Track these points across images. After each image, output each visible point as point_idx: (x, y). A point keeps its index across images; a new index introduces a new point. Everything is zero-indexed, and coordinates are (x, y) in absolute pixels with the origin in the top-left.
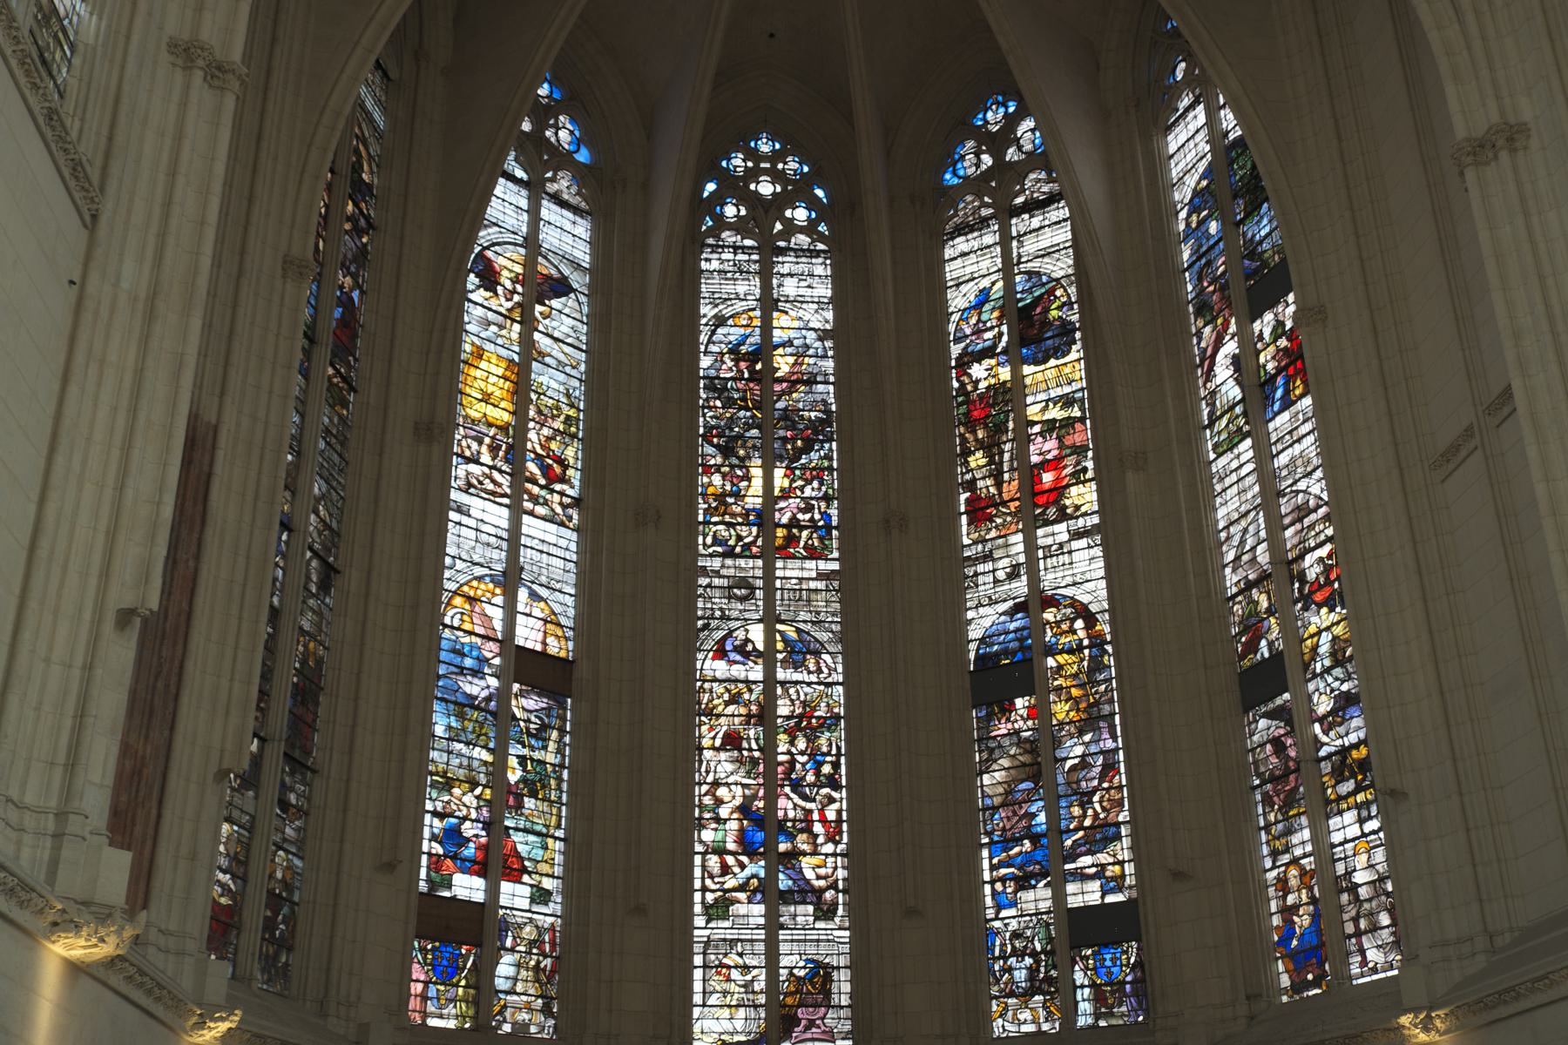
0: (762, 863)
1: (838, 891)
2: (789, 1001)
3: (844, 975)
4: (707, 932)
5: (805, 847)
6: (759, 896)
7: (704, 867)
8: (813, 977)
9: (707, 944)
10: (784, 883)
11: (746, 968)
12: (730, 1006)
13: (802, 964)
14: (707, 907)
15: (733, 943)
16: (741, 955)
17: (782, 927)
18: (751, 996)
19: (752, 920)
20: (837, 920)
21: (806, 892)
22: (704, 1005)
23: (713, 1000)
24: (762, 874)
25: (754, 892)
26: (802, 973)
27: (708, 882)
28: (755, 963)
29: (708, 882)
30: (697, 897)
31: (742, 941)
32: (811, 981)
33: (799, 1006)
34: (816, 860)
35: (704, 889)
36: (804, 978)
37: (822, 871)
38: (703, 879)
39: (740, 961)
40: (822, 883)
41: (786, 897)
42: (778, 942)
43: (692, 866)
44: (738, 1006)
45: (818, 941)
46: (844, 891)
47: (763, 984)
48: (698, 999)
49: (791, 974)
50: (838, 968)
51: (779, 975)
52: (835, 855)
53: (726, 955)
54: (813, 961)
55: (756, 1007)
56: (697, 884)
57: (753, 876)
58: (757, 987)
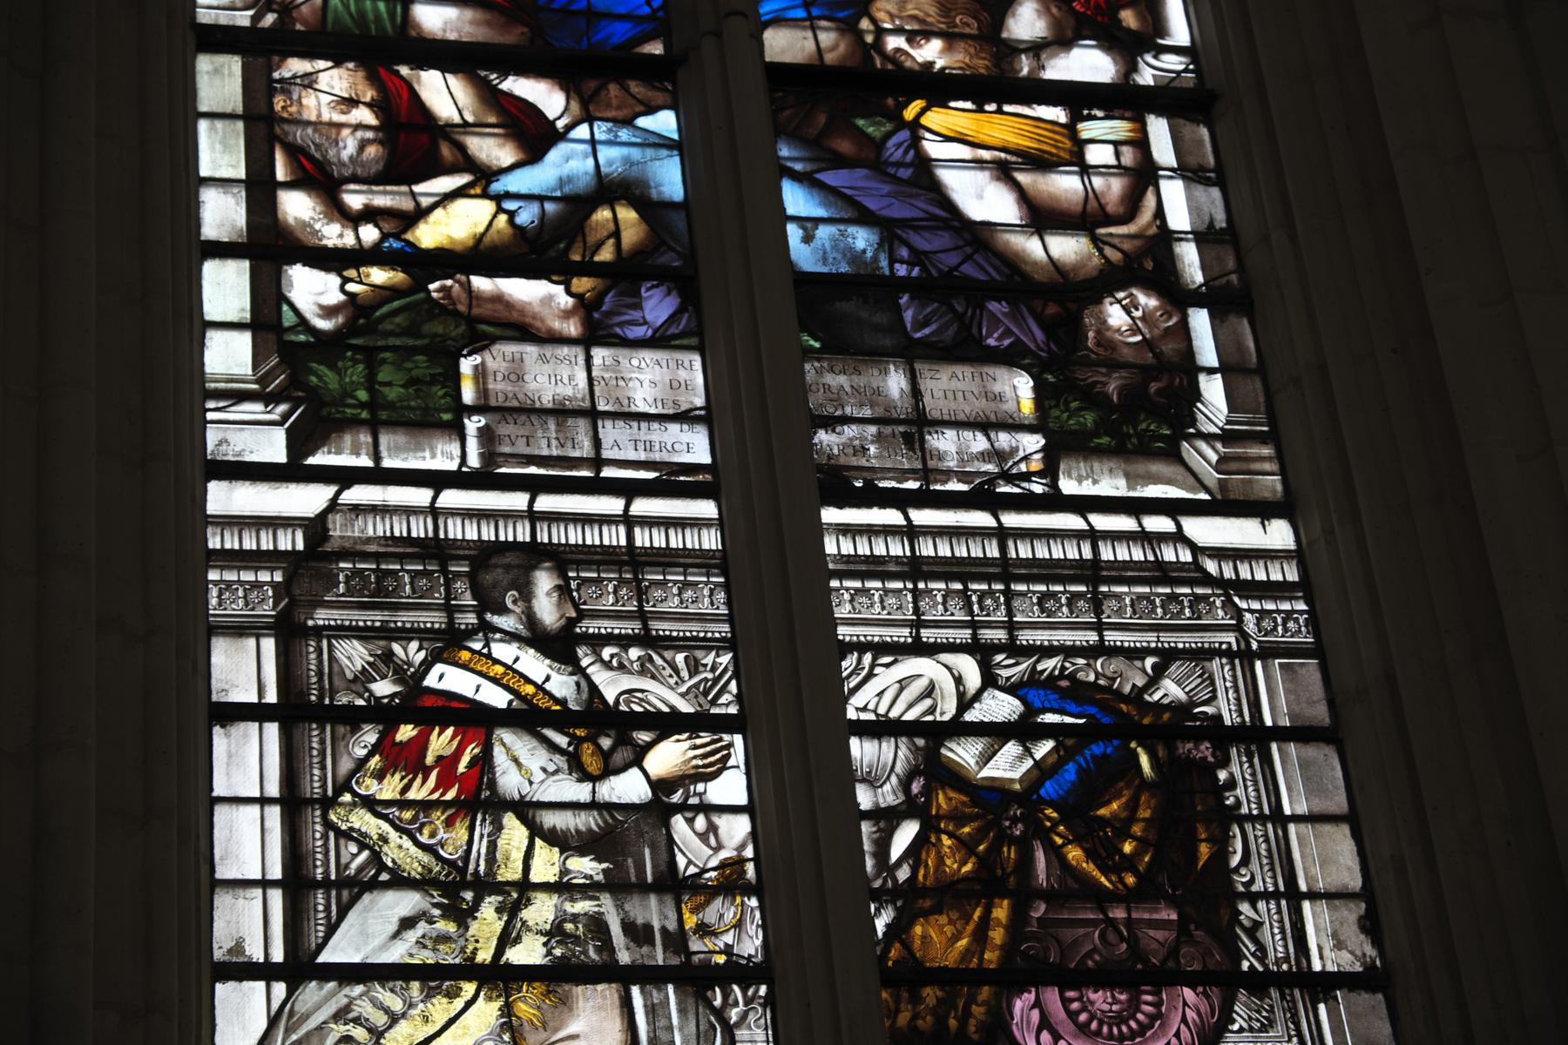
0: (665, 122)
1: (1178, 297)
2: (941, 940)
3: (1300, 782)
4: (308, 499)
5: (931, 52)
6: (657, 307)
7: (263, 124)
8: (1094, 787)
9: (314, 559)
10: (813, 230)
11: (600, 733)
12: (499, 977)
13: (1000, 707)
14: (296, 365)
15: (497, 569)
16: (558, 645)
17: (841, 486)
18: (654, 912)
19: (618, 441)
20: (1203, 457)
21: (978, 293)
22: (299, 967)
23: (369, 932)
24: (669, 178)
25: (628, 275)
26: (1008, 765)
27: (297, 206)
28: (665, 696)
29: (297, 206)
30: (225, 289)
31: (562, 559)
32: (1078, 813)
33: (1019, 973)
34: (1005, 127)
35: (269, 248)
36: (1029, 794)
37: (1065, 185)
38: (259, 190)
39: (562, 685)
40: (1067, 247)
41: (846, 315)
42: (819, 573)
43: (183, 115)
44: (560, 976)
45: (1092, 572)
46: (1216, 299)
47: (736, 829)
48: (247, 924)
49: (933, 770)
50: (1255, 737)
51: (847, 776)
52: (1120, 99)
53: (447, 645)
54: (1071, 692)
55: (697, 979)
56: (221, 214)
57: (607, 190)
58: (691, 848)
